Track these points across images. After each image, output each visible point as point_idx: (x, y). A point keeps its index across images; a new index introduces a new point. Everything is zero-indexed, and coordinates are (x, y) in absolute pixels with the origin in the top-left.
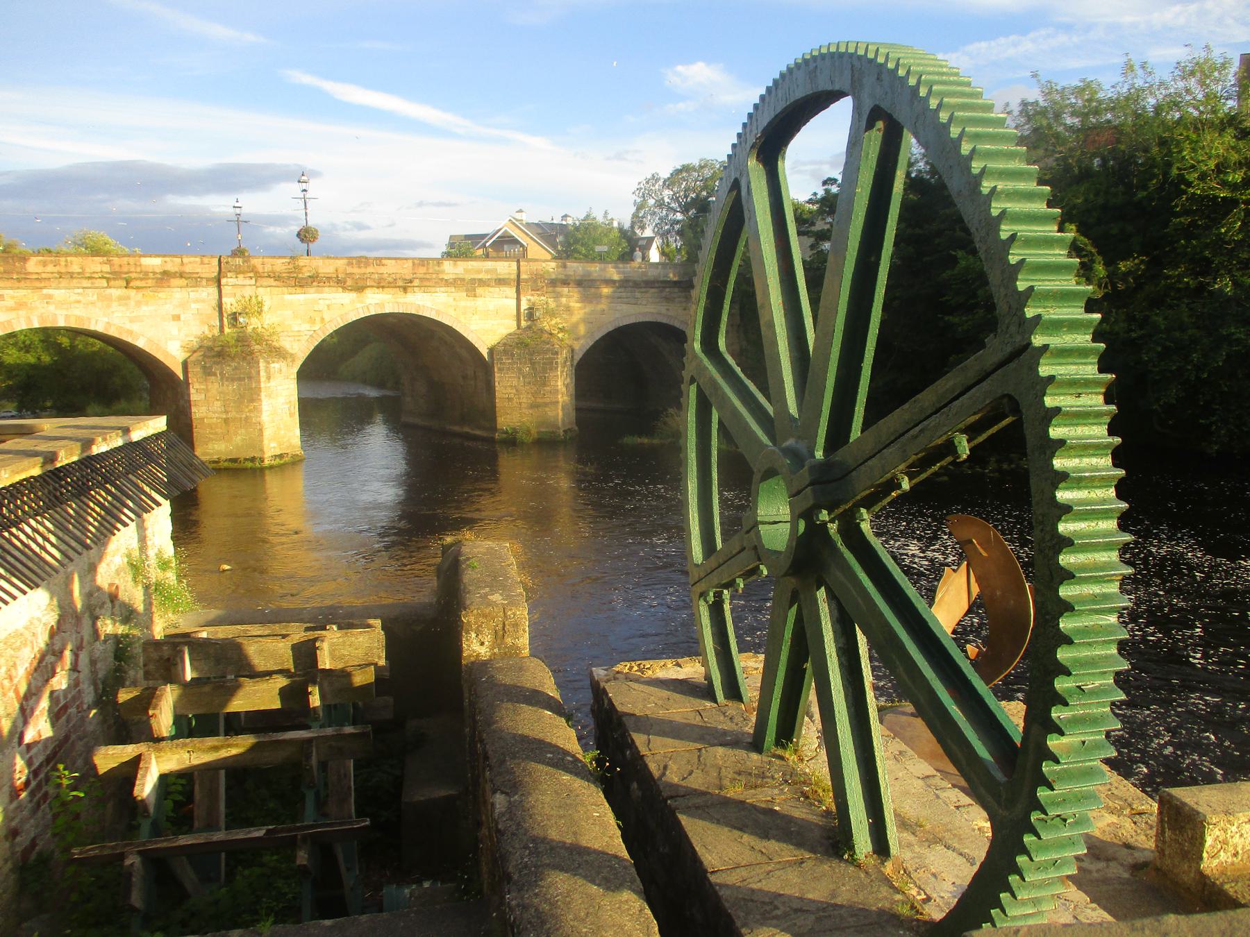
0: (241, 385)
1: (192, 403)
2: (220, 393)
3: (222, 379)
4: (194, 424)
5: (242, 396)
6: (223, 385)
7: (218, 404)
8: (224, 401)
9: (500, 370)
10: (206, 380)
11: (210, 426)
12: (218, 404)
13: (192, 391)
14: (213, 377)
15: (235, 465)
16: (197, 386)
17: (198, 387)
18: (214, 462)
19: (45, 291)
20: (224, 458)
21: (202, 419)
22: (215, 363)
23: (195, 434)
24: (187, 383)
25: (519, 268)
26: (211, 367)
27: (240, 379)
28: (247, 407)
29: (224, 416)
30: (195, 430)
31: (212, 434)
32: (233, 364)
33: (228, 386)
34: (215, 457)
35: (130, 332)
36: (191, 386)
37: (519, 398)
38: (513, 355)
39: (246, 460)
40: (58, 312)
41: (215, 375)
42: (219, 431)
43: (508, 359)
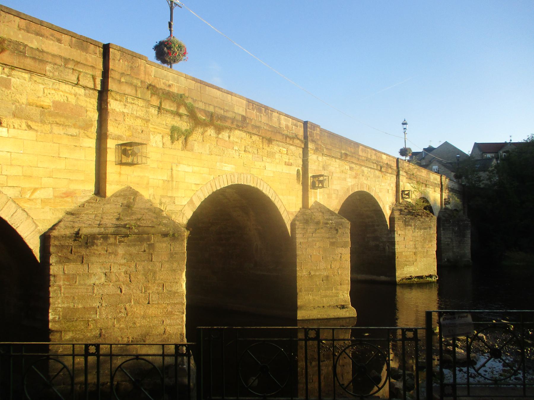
0: (425, 232)
1: (396, 243)
2: (413, 237)
3: (414, 229)
4: (397, 256)
5: (425, 239)
6: (415, 231)
7: (411, 243)
8: (415, 241)
9: (444, 229)
10: (405, 229)
11: (406, 256)
12: (411, 243)
13: (396, 235)
14: (410, 227)
15: (421, 280)
16: (399, 232)
17: (400, 233)
18: (409, 279)
19: (363, 168)
20: (413, 275)
21: (401, 253)
22: (411, 219)
23: (396, 262)
24: (392, 230)
25: (441, 179)
26: (408, 222)
27: (425, 229)
28: (428, 245)
29: (414, 251)
30: (397, 260)
31: (407, 261)
32: (421, 219)
33: (417, 232)
34: (408, 276)
35: (379, 198)
36: (396, 233)
37: (452, 244)
38: (450, 222)
39: (427, 277)
40: (365, 182)
41: (411, 226)
42: (411, 259)
43: (448, 224)
